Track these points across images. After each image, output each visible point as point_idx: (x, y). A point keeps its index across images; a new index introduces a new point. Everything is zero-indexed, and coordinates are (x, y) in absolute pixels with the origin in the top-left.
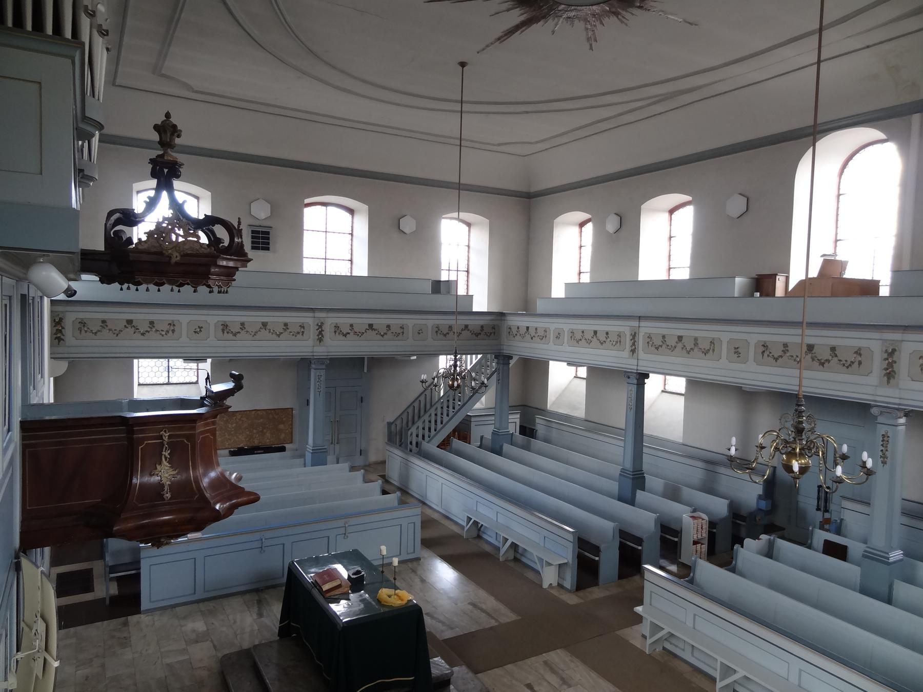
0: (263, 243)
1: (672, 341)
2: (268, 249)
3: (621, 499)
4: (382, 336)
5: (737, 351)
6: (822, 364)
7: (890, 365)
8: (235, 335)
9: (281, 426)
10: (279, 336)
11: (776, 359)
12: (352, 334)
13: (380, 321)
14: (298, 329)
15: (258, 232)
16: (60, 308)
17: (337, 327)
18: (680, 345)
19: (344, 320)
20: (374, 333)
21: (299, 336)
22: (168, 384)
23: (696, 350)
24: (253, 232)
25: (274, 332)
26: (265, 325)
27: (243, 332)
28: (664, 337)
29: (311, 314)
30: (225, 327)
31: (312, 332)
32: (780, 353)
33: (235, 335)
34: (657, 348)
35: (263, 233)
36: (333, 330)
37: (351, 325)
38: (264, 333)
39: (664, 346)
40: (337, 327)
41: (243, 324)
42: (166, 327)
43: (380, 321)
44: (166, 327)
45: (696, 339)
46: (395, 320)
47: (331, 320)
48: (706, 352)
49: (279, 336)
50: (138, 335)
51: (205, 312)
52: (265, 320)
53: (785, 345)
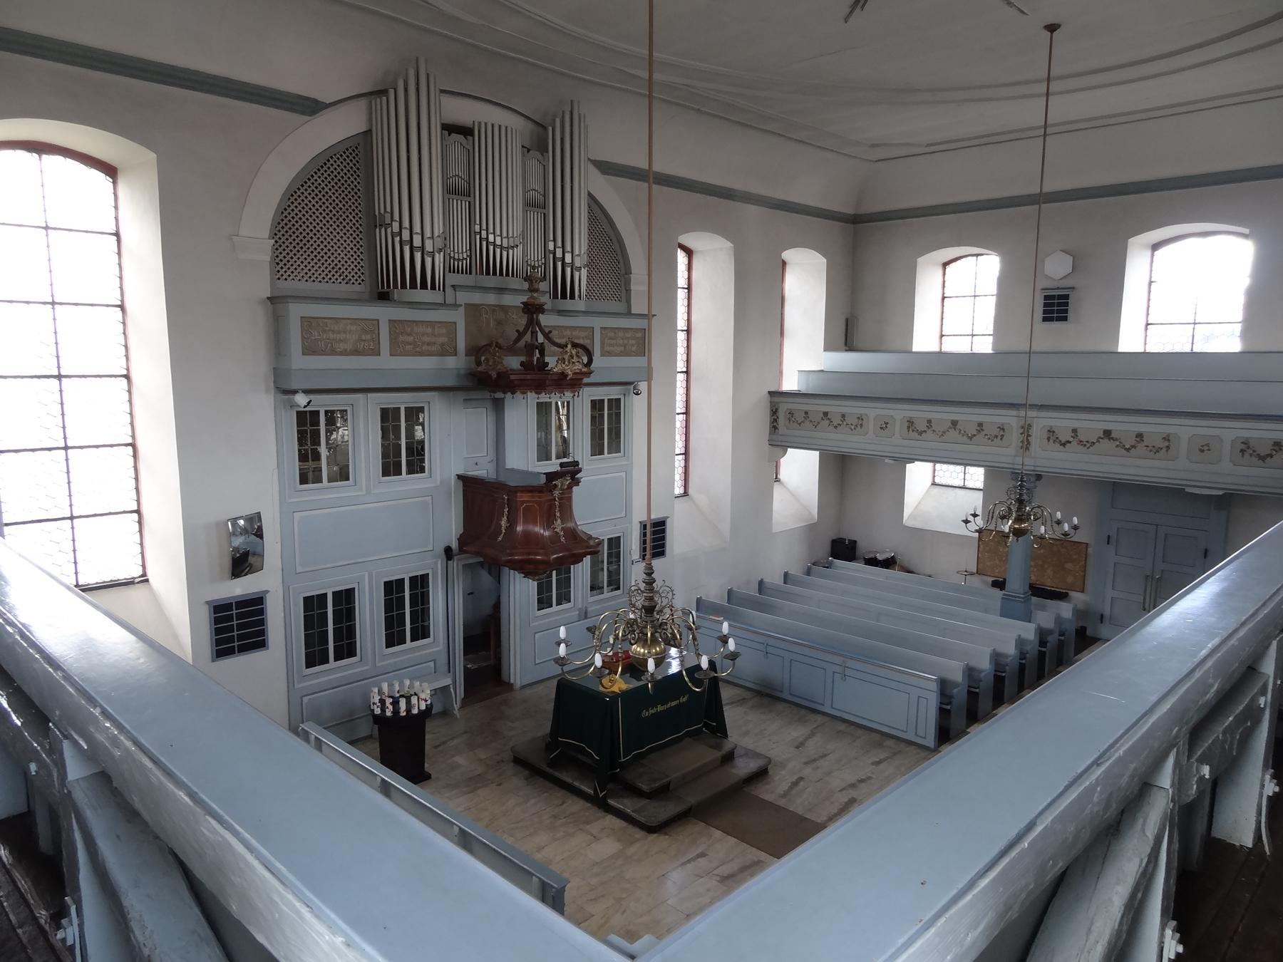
0: (1059, 311)
2: (1065, 319)
4: (1128, 450)
8: (920, 434)
9: (1069, 566)
10: (971, 438)
12: (1074, 443)
13: (1124, 426)
14: (996, 432)
15: (1052, 297)
16: (776, 399)
17: (1051, 431)
19: (1063, 423)
20: (1113, 444)
21: (997, 441)
22: (964, 487)
24: (1046, 297)
25: (965, 434)
26: (954, 423)
27: (929, 432)
29: (1014, 413)
30: (911, 424)
31: (1014, 437)
33: (920, 434)
35: (1060, 297)
36: (1045, 435)
37: (1075, 431)
38: (953, 434)
40: (1051, 431)
41: (929, 421)
42: (855, 421)
43: (1124, 426)
44: (855, 421)
46: (1153, 428)
47: (1042, 422)
49: (971, 438)
50: (831, 428)
51: (865, 404)
52: (955, 417)
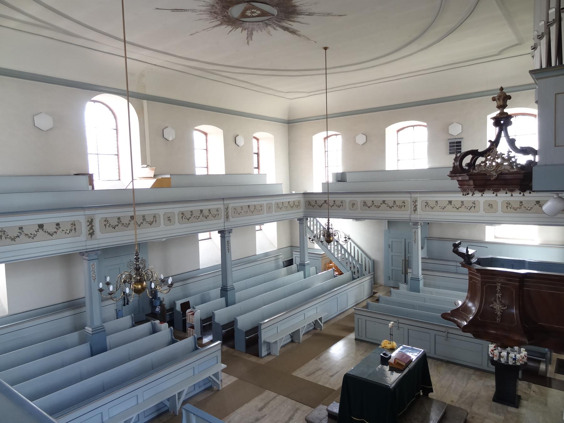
1: (206, 213)
3: (93, 353)
5: (169, 220)
6: (206, 218)
7: (227, 213)
11: (188, 219)
18: (132, 222)
23: (144, 223)
28: (119, 218)
32: (190, 216)
34: (114, 228)
39: (120, 225)
45: (144, 216)
48: (151, 224)
53: (192, 212)
